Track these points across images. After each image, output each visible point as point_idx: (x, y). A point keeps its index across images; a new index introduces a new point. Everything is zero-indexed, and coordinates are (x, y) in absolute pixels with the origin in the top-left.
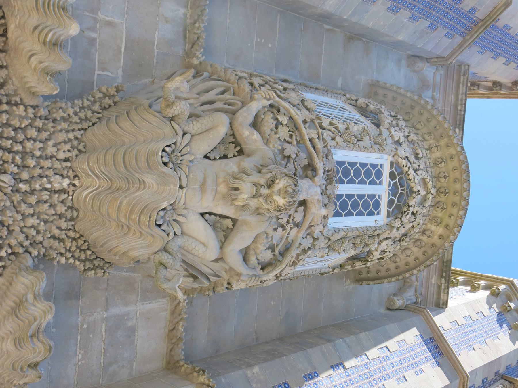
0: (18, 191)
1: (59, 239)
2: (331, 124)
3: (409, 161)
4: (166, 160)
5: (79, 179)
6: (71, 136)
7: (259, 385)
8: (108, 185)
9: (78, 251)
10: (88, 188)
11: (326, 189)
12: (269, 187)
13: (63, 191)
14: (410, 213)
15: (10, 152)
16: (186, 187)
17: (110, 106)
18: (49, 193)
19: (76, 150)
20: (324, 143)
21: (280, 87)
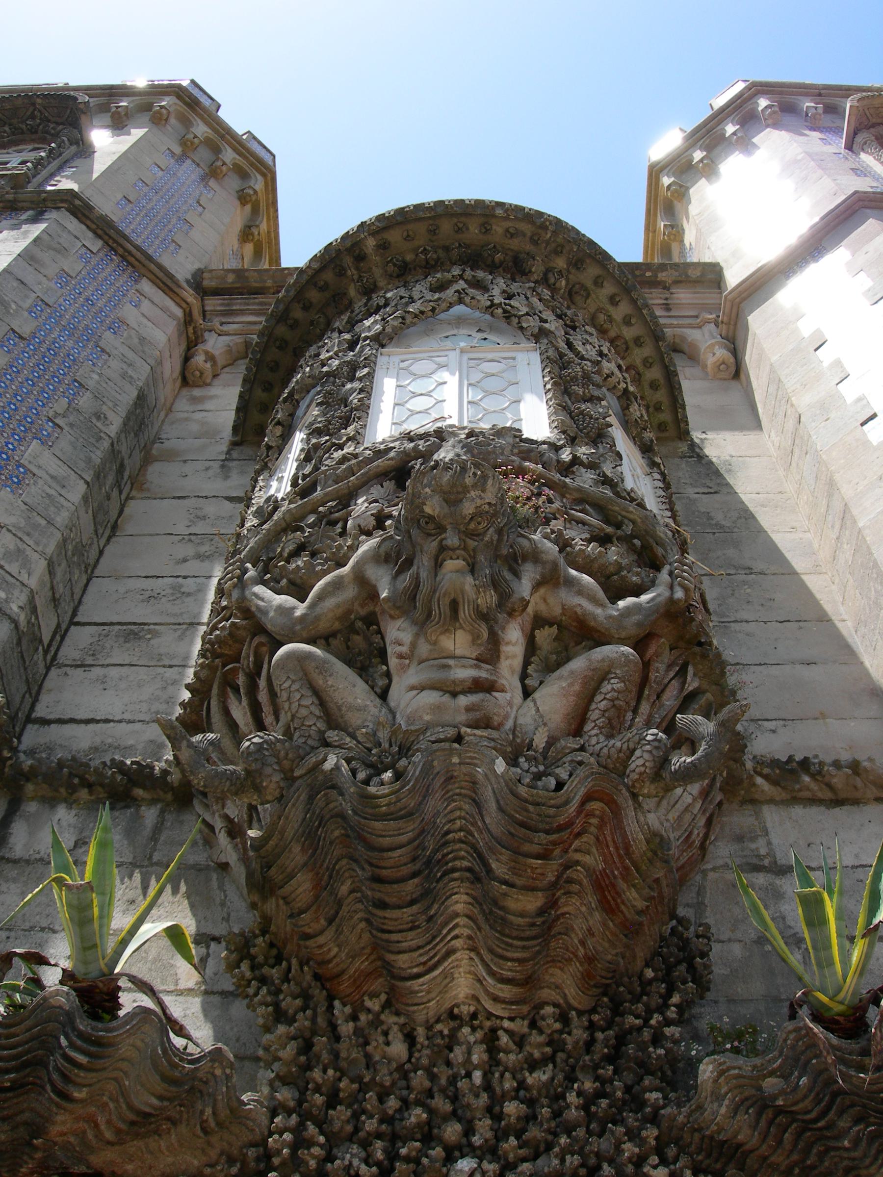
6: (346, 1028)
12: (441, 529)
13: (491, 1040)
17: (272, 945)
19: (383, 1017)
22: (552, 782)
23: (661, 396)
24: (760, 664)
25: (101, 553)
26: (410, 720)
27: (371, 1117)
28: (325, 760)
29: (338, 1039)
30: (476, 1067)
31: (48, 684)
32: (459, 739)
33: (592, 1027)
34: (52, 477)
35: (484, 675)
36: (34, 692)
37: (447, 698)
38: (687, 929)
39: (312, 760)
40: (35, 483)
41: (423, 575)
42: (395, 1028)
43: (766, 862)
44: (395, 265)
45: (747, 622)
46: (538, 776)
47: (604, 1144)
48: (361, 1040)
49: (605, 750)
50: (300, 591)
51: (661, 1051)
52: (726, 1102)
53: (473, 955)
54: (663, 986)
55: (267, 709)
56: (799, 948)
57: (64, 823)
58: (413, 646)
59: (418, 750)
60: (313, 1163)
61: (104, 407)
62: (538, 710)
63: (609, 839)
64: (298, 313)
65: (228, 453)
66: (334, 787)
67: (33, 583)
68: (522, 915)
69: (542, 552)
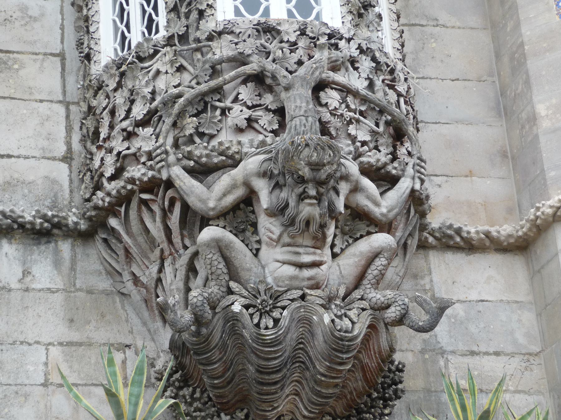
4: (271, 324)
5: (283, 415)
9: (373, 410)
11: (288, 41)
24: (436, 123)
28: (233, 304)
35: (317, 258)
39: (225, 303)
41: (292, 203)
45: (430, 78)
46: (340, 317)
49: (374, 300)
50: (202, 171)
53: (297, 398)
54: (381, 402)
56: (443, 357)
57: (11, 257)
62: (341, 273)
63: (371, 347)
69: (351, 175)
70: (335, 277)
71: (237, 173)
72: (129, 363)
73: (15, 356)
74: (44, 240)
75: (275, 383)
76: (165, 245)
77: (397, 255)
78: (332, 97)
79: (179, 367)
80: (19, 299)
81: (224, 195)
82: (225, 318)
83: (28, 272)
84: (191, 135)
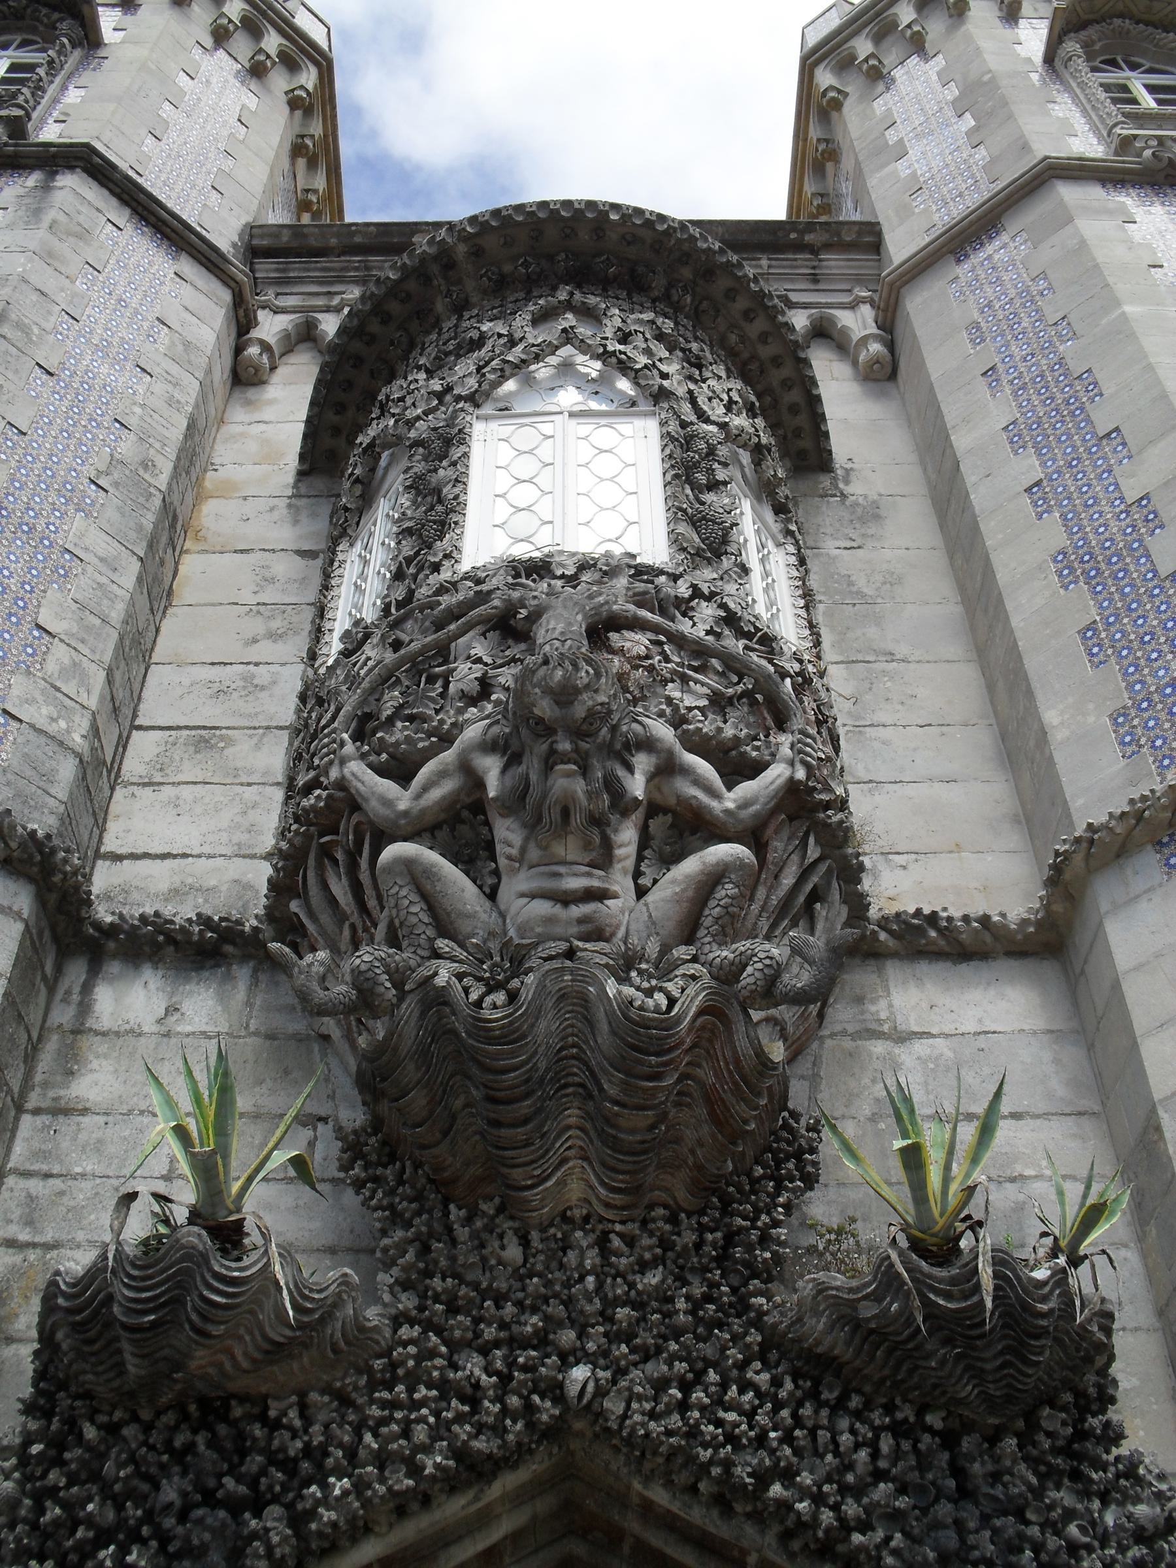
0: (606, 1354)
1: (725, 1248)
2: (398, 576)
3: (487, 363)
6: (462, 1233)
7: (1091, 706)
8: (578, 1137)
10: (592, 1187)
11: (563, 576)
13: (603, 1242)
14: (622, 347)
15: (510, 1378)
16: (567, 941)
17: (384, 1143)
18: (609, 1280)
20: (447, 591)
21: (314, 715)
22: (664, 1003)
23: (802, 420)
25: (158, 630)
26: (522, 930)
27: (489, 1325)
28: (436, 974)
29: (454, 1242)
30: (588, 1273)
31: (113, 808)
32: (570, 954)
33: (702, 1229)
34: (102, 560)
35: (596, 883)
36: (100, 821)
37: (558, 909)
38: (797, 1122)
40: (84, 571)
41: (534, 778)
42: (510, 1233)
43: (886, 1028)
44: (490, 279)
46: (649, 993)
47: (708, 1350)
48: (476, 1242)
50: (401, 770)
51: (768, 1255)
52: (823, 1320)
53: (585, 1164)
55: (369, 892)
58: (523, 850)
59: (531, 970)
60: (435, 1374)
61: (152, 451)
62: (650, 916)
64: (375, 327)
65: (295, 486)
66: (446, 1003)
67: (93, 703)
68: (632, 1131)
69: (658, 740)
70: (641, 927)
71: (448, 756)
72: (319, 1146)
73: (127, 1133)
74: (212, 962)
75: (525, 1121)
76: (355, 918)
77: (794, 924)
78: (636, 642)
79: (376, 1124)
80: (152, 1046)
81: (425, 789)
82: (421, 1001)
83: (177, 1010)
84: (390, 721)
